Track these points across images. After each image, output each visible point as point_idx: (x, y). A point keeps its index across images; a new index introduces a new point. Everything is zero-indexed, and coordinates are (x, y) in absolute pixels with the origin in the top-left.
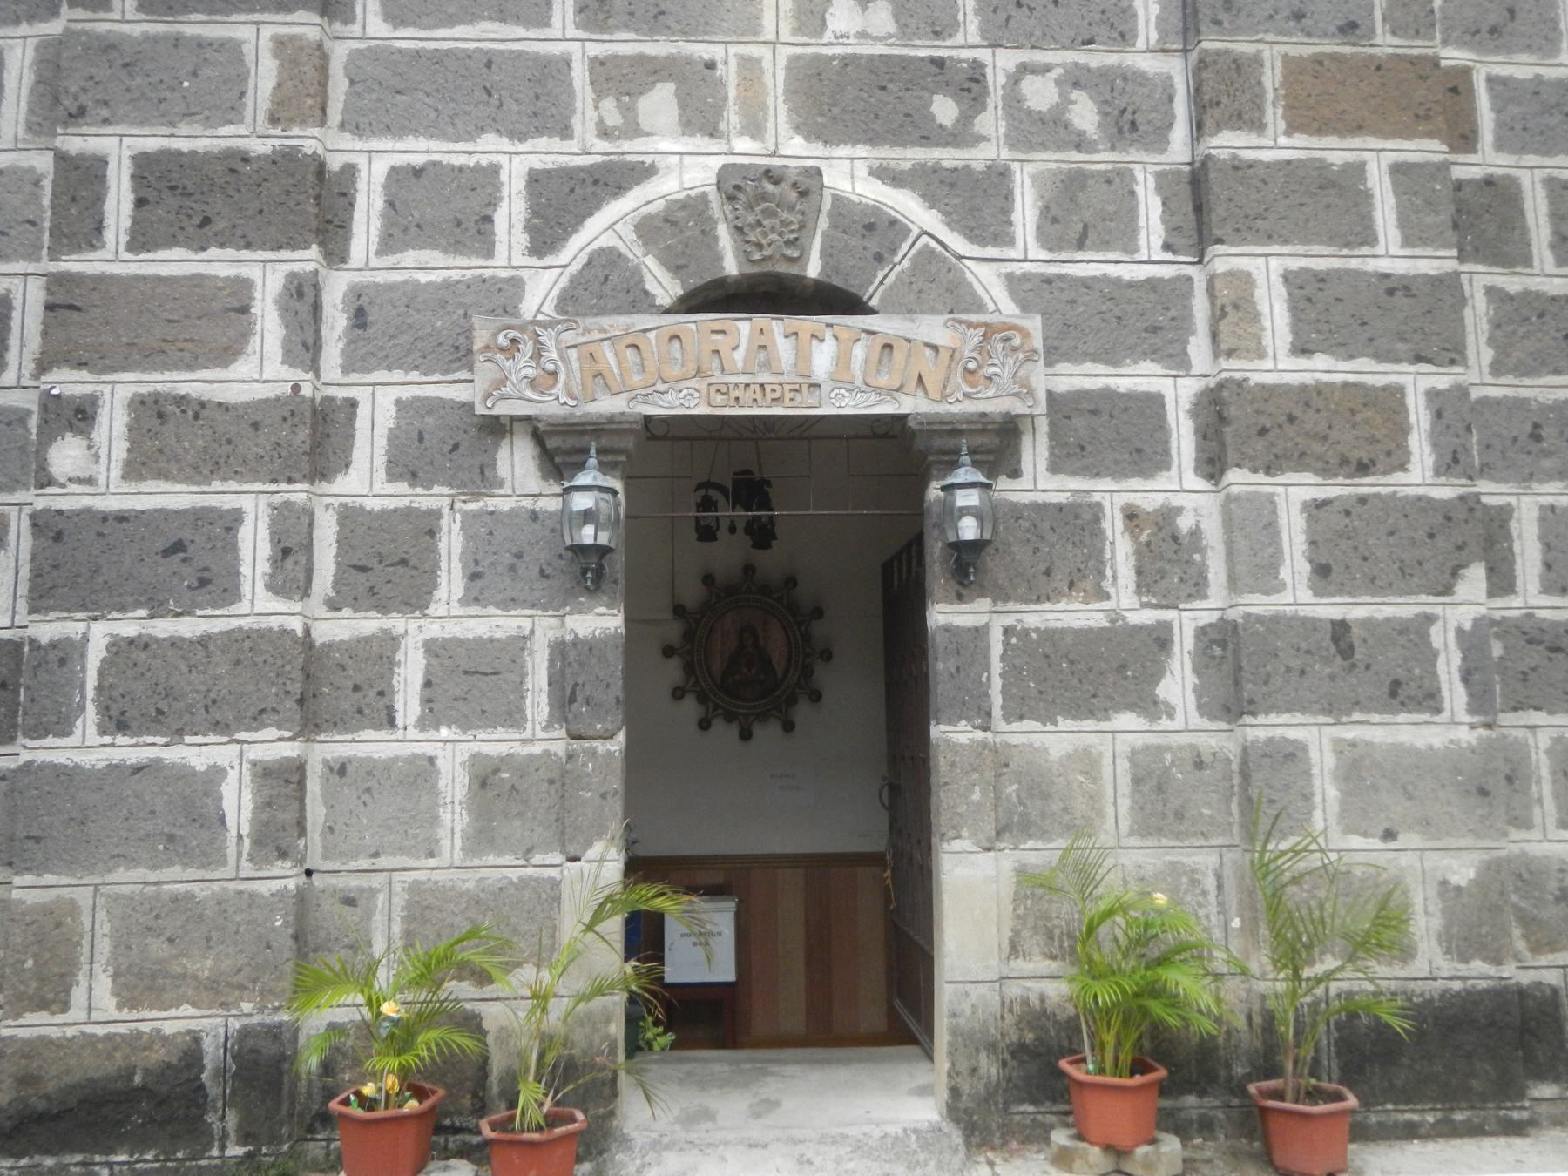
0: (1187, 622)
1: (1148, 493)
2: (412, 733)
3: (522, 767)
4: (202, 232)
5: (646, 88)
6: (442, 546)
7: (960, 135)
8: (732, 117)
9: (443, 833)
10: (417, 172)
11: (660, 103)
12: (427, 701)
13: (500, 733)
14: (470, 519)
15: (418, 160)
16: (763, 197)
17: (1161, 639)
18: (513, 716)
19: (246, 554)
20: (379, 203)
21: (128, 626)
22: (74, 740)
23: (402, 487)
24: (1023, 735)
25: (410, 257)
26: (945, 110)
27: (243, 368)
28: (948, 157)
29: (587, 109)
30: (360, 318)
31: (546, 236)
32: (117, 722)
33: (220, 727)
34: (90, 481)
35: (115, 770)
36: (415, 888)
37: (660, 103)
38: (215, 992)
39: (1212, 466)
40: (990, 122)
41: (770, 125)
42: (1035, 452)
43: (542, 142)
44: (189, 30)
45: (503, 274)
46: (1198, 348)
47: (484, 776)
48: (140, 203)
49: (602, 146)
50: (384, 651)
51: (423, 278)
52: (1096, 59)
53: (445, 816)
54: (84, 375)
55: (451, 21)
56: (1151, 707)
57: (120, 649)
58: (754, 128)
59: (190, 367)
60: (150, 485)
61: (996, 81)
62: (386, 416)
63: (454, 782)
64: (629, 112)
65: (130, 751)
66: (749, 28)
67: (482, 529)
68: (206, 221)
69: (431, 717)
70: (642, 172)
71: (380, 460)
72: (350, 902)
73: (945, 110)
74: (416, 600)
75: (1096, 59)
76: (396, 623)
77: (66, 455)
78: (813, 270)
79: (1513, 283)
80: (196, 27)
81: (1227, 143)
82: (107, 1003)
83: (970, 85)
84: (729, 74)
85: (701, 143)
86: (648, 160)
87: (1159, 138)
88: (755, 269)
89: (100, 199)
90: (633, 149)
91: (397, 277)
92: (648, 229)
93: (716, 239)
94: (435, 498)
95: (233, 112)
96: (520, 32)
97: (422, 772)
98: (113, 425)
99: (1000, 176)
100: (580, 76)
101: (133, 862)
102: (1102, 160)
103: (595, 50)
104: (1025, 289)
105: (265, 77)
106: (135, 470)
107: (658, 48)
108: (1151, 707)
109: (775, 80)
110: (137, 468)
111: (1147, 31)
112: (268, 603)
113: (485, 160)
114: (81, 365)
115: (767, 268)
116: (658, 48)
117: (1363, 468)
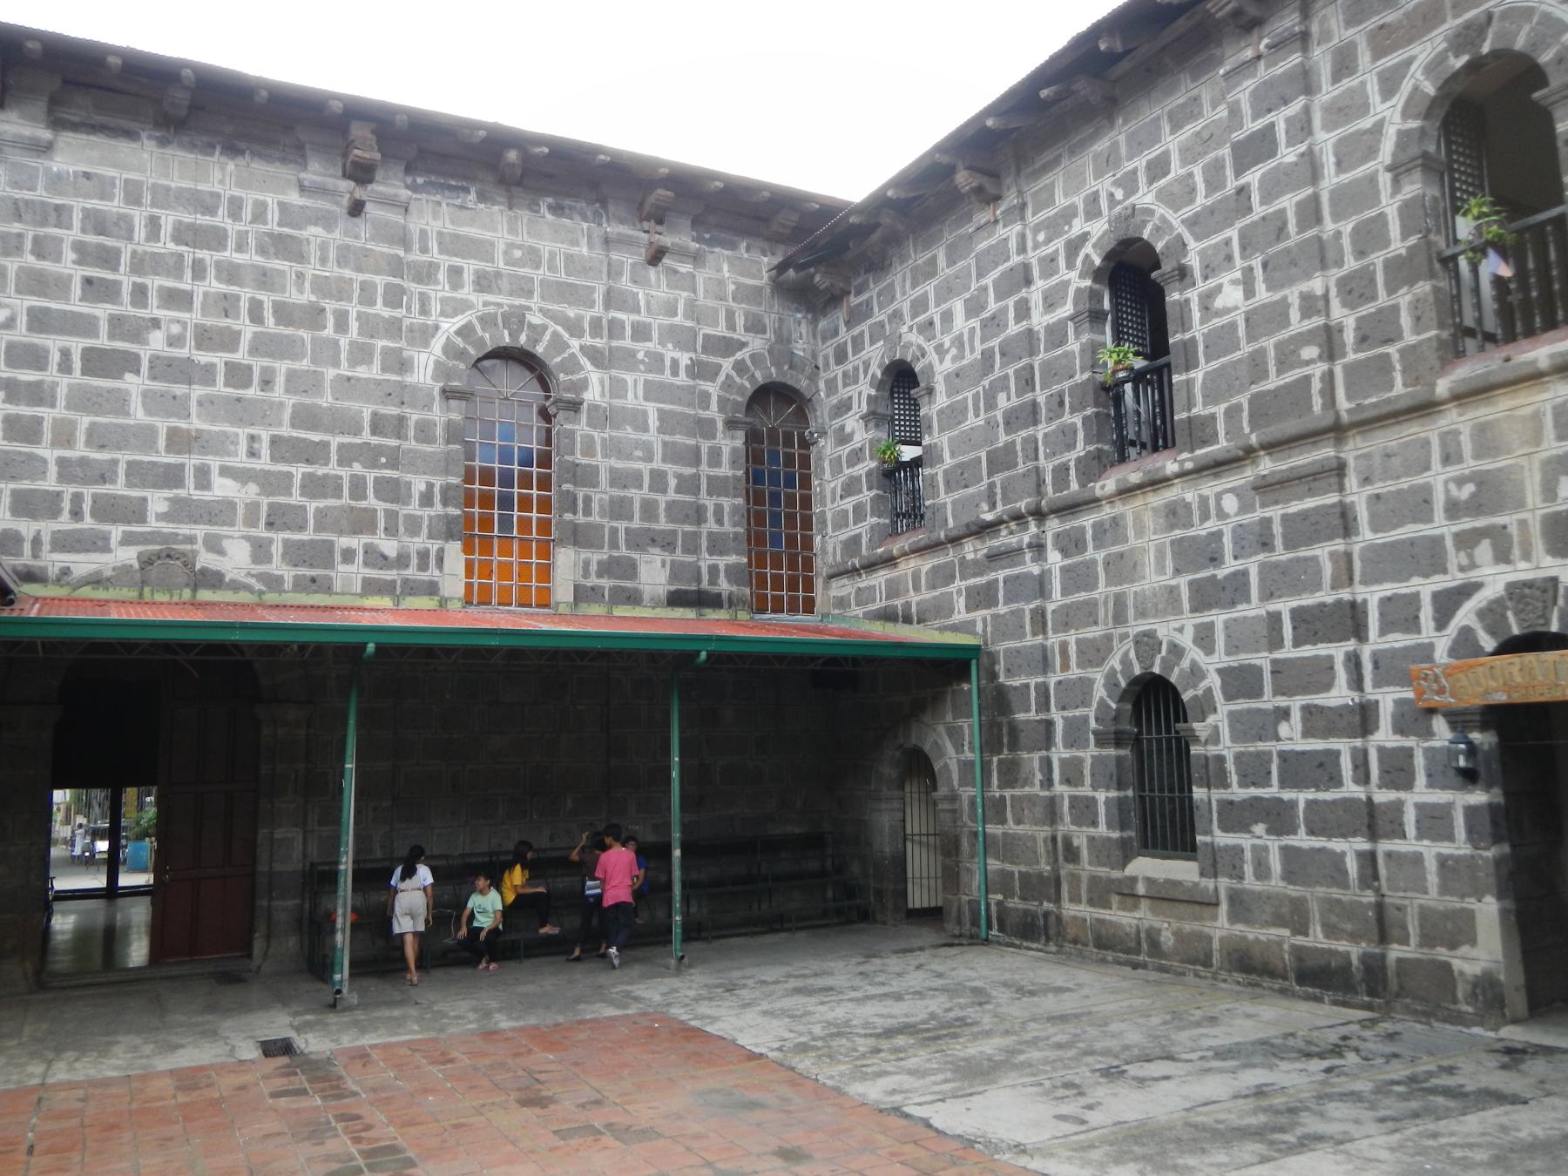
2: (1414, 842)
3: (1457, 859)
5: (1477, 543)
6: (1416, 762)
8: (1516, 552)
9: (1429, 885)
10: (1389, 599)
11: (1484, 550)
12: (1418, 828)
13: (1446, 844)
14: (1427, 751)
15: (1389, 593)
16: (1524, 596)
19: (1343, 768)
20: (1377, 615)
22: (1298, 837)
23: (1398, 737)
25: (1391, 637)
27: (1334, 692)
29: (1454, 558)
30: (1376, 665)
31: (1441, 622)
33: (1344, 836)
34: (1291, 739)
36: (1421, 907)
37: (1484, 550)
38: (1354, 937)
41: (1534, 553)
43: (1436, 578)
44: (1301, 554)
45: (1426, 641)
47: (1443, 861)
48: (1294, 628)
49: (1461, 575)
51: (1397, 645)
53: (1429, 877)
54: (1285, 698)
55: (1395, 527)
58: (1527, 556)
59: (1317, 693)
60: (1311, 740)
64: (1470, 557)
66: (1520, 504)
67: (1430, 754)
68: (1316, 633)
70: (1477, 586)
71: (1390, 726)
72: (1399, 909)
76: (1402, 795)
77: (1283, 729)
78: (1554, 627)
80: (1304, 553)
84: (1514, 530)
85: (1503, 567)
86: (1479, 580)
88: (1526, 631)
89: (1281, 628)
90: (1473, 576)
91: (1387, 646)
93: (1507, 618)
94: (1410, 742)
96: (1422, 526)
98: (1296, 716)
100: (1449, 543)
101: (1322, 885)
103: (1455, 529)
105: (1328, 570)
106: (1307, 733)
109: (1536, 530)
110: (1307, 733)
112: (1354, 788)
113: (1413, 590)
114: (1284, 694)
115: (1531, 630)
116: (1481, 522)
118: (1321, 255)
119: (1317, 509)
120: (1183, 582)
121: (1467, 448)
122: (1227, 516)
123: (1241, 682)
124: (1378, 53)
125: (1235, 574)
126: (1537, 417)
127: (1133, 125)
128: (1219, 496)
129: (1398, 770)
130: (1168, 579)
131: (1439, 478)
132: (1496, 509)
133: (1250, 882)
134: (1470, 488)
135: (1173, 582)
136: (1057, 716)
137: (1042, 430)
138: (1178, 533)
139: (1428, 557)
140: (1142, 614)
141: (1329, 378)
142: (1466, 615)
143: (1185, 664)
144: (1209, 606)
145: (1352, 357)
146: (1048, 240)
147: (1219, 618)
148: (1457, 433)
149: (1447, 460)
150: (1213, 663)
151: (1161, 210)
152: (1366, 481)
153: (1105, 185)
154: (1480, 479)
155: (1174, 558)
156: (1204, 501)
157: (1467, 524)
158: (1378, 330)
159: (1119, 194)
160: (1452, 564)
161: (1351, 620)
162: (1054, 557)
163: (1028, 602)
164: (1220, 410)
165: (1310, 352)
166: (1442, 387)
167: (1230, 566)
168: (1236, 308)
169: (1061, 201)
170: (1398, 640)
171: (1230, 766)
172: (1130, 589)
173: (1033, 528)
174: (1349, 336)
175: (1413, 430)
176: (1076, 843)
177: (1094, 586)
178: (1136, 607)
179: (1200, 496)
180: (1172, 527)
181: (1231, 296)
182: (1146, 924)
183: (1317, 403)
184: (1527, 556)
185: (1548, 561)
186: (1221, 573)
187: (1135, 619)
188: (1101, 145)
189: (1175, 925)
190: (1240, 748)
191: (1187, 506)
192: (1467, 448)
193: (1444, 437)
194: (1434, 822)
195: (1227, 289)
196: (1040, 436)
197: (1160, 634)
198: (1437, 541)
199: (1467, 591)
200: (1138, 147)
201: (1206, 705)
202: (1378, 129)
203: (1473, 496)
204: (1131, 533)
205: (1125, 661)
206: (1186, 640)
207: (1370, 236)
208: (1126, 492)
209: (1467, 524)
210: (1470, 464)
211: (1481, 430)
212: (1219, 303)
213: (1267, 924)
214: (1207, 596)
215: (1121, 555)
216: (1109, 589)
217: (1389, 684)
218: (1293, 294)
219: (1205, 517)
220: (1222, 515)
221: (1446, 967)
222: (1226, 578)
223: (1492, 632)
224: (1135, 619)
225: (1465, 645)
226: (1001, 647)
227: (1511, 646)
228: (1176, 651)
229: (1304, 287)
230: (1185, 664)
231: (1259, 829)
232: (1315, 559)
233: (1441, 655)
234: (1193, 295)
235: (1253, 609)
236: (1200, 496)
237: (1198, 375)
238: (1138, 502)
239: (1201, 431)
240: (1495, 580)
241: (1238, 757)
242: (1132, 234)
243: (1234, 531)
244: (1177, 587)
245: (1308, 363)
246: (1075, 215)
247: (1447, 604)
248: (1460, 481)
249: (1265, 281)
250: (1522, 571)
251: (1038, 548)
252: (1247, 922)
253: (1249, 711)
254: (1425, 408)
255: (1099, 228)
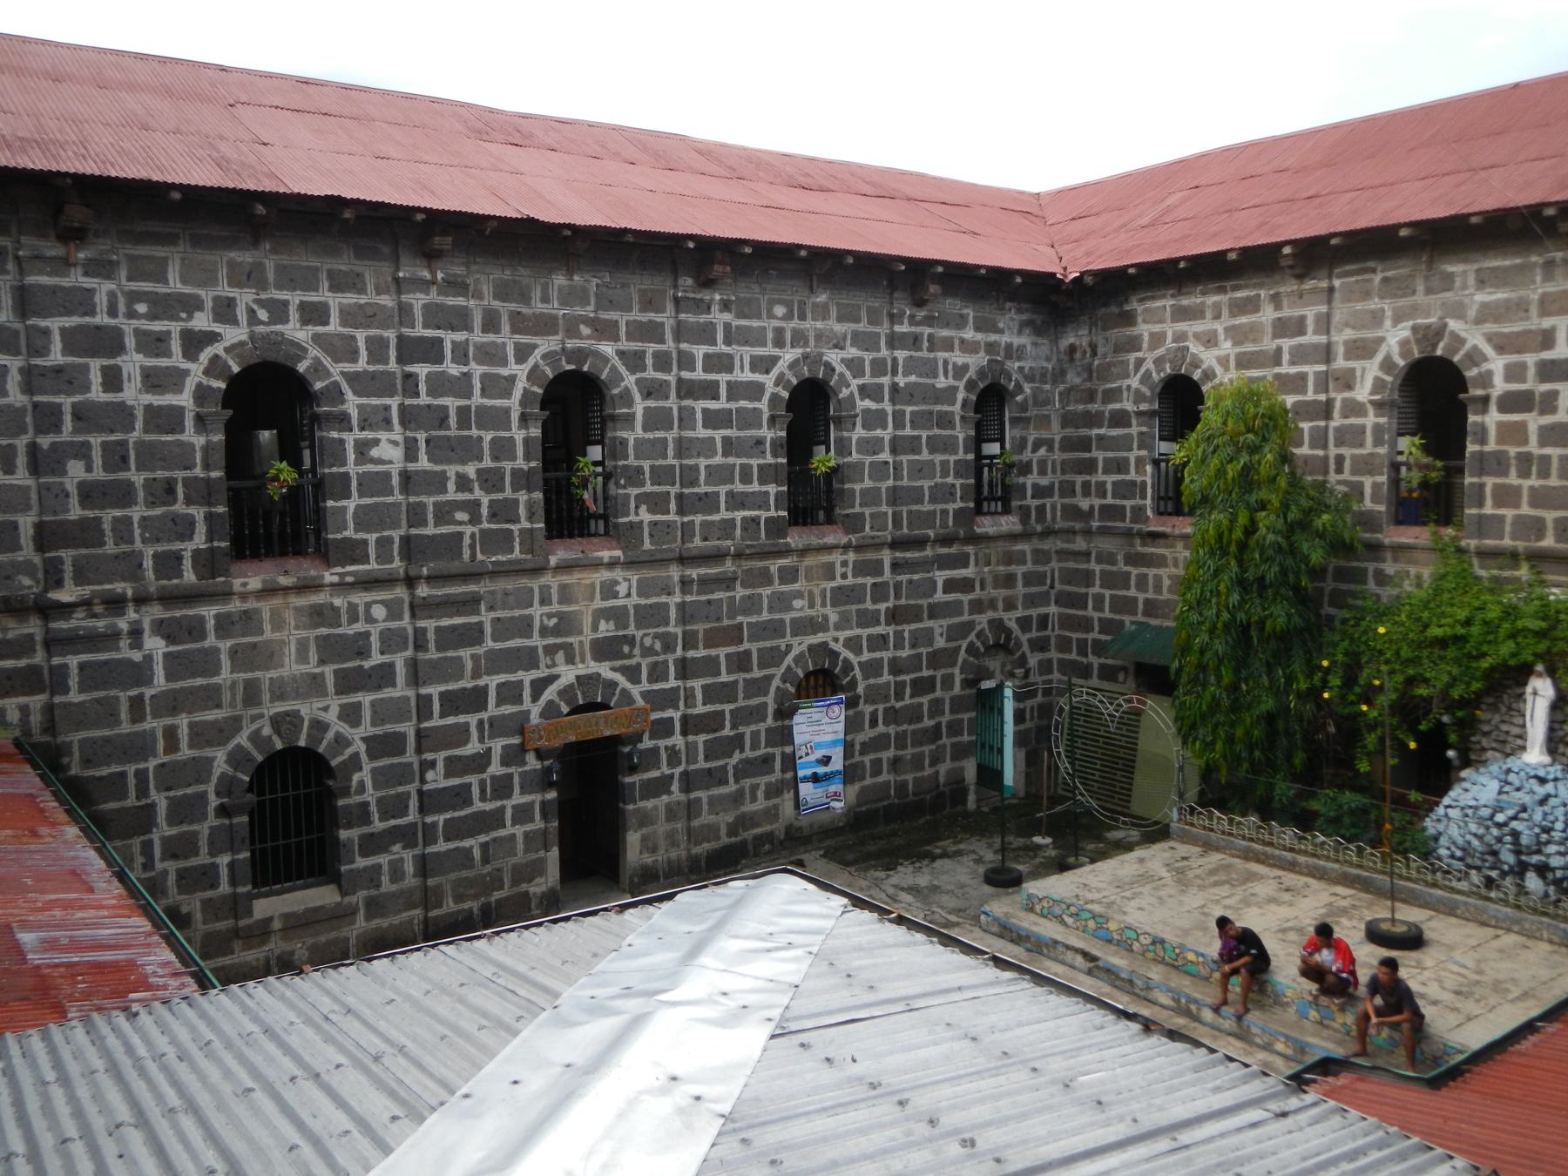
0: (678, 771)
1: (669, 742)
4: (457, 711)
7: (630, 656)
8: (578, 659)
11: (560, 656)
17: (672, 776)
18: (532, 820)
21: (448, 816)
24: (641, 804)
26: (626, 649)
27: (470, 746)
28: (627, 662)
29: (544, 660)
31: (535, 698)
32: (447, 839)
35: (449, 851)
37: (560, 657)
38: (476, 897)
39: (684, 733)
40: (637, 651)
42: (646, 736)
46: (681, 704)
50: (502, 809)
52: (661, 630)
56: (669, 793)
57: (446, 821)
58: (583, 661)
61: (638, 639)
62: (499, 750)
63: (520, 839)
65: (451, 845)
66: (580, 633)
69: (513, 825)
70: (555, 678)
73: (626, 649)
74: (509, 796)
75: (661, 630)
77: (430, 775)
79: (748, 676)
80: (450, 654)
81: (691, 654)
82: (451, 904)
83: (631, 641)
84: (576, 646)
87: (674, 651)
90: (555, 671)
92: (561, 693)
95: (461, 677)
97: (513, 836)
98: (440, 765)
99: (639, 665)
102: (661, 658)
104: (644, 695)
105: (469, 665)
106: (447, 776)
107: (559, 640)
108: (669, 793)
109: (587, 647)
111: (673, 622)
116: (559, 640)
117: (716, 731)
118: (469, 450)
119: (463, 625)
120: (328, 671)
121: (555, 598)
122: (376, 621)
123: (382, 746)
124: (515, 330)
125: (381, 666)
126: (593, 585)
127: (285, 259)
128: (368, 605)
129: (502, 788)
130: (312, 667)
131: (537, 611)
132: (569, 634)
133: (387, 886)
134: (554, 621)
135: (317, 670)
136: (161, 801)
137: (137, 513)
138: (324, 631)
139: (528, 659)
140: (279, 693)
141: (473, 536)
142: (550, 693)
143: (330, 735)
144: (355, 689)
145: (485, 525)
146: (152, 317)
147: (366, 699)
148: (549, 587)
149: (543, 602)
150: (357, 737)
151: (314, 352)
152: (491, 608)
153: (245, 298)
154: (561, 616)
155: (318, 651)
156: (352, 608)
157: (551, 641)
158: (504, 511)
159: (263, 315)
160: (542, 665)
161: (476, 700)
162: (155, 645)
163: (124, 689)
164: (372, 538)
165: (461, 516)
166: (553, 561)
167: (376, 659)
168: (391, 462)
169: (175, 284)
170: (508, 709)
171: (373, 808)
172: (266, 676)
173: (132, 615)
174: (485, 511)
175: (524, 582)
176: (185, 909)
177: (217, 672)
178: (271, 691)
179: (350, 603)
180: (317, 625)
181: (389, 450)
182: (277, 952)
183: (466, 554)
184: (583, 661)
185: (592, 664)
186: (367, 664)
187: (272, 701)
188: (245, 257)
189: (310, 941)
190: (379, 794)
191: (336, 610)
192: (555, 598)
193: (541, 587)
194: (522, 814)
195: (383, 444)
196: (136, 519)
197: (303, 713)
198: (534, 649)
199: (552, 679)
200: (289, 280)
201: (354, 763)
202: (512, 379)
203: (556, 625)
204: (267, 627)
205: (255, 737)
206: (332, 716)
207: (502, 449)
208: (269, 591)
209: (551, 641)
210: (556, 607)
211: (563, 588)
212: (375, 452)
213: (400, 911)
214: (347, 682)
215: (254, 646)
216: (235, 675)
217: (499, 736)
218: (452, 470)
219: (353, 619)
220: (370, 619)
221: (526, 894)
222: (372, 668)
223: (568, 704)
224: (272, 701)
225: (550, 711)
226: (76, 737)
227: (577, 710)
228: (319, 726)
229: (460, 469)
230: (330, 735)
231: (397, 848)
232: (460, 658)
233: (535, 718)
234: (350, 439)
235: (400, 690)
236: (350, 603)
237: (351, 505)
238: (277, 601)
239: (354, 552)
240: (568, 674)
241: (380, 801)
242: (281, 359)
243: (381, 633)
244: (322, 674)
245: (461, 523)
246: (200, 308)
247: (539, 686)
248: (550, 616)
249: (427, 453)
250: (582, 669)
251: (136, 633)
252: (383, 915)
253: (392, 766)
254: (538, 570)
255: (234, 334)
